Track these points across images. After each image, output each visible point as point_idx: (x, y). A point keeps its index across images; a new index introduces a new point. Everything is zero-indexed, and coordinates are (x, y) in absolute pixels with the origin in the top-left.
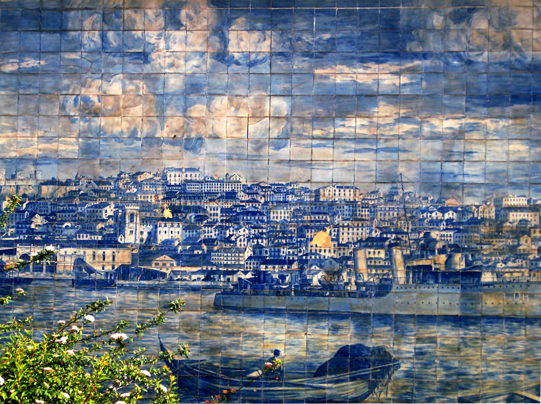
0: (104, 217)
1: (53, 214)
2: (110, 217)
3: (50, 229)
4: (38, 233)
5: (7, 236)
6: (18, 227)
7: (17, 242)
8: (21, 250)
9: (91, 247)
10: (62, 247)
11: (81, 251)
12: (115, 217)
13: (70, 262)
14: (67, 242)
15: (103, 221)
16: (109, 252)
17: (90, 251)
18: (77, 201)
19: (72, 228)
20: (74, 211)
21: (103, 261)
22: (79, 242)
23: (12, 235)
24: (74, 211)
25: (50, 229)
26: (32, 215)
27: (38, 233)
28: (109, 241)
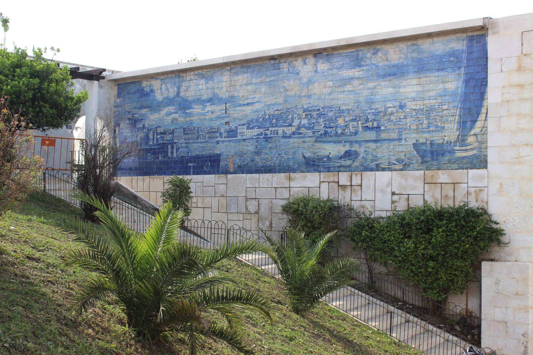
8: (270, 129)
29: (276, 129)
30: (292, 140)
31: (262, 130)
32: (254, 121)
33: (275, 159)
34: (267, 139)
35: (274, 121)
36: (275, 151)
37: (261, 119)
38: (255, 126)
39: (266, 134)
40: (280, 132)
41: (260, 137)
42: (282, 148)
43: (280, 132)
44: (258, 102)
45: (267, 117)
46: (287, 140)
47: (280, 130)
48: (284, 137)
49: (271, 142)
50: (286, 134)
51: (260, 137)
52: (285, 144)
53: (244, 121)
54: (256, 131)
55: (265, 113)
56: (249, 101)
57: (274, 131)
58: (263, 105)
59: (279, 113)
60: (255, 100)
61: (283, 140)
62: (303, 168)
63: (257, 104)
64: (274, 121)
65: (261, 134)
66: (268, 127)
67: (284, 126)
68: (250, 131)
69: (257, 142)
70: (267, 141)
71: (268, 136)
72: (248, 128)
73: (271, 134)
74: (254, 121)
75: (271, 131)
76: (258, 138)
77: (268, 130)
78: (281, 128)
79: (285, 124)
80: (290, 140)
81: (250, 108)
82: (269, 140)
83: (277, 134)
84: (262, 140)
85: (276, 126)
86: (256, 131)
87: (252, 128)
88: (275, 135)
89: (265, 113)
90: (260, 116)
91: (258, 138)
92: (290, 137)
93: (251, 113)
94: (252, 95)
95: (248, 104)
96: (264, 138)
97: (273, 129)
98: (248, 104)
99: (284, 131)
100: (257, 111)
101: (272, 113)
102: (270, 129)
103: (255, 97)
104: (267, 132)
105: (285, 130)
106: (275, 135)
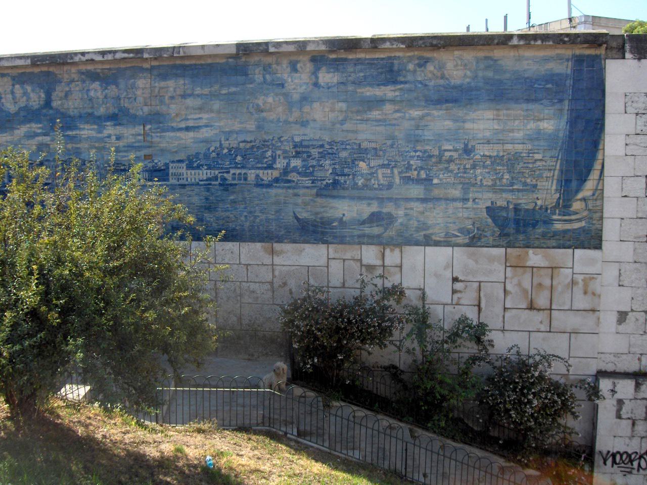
8: (232, 171)
26: (236, 156)
31: (217, 172)
32: (201, 156)
37: (214, 155)
38: (202, 165)
41: (213, 183)
45: (225, 151)
51: (213, 183)
53: (182, 156)
55: (221, 144)
64: (239, 158)
65: (216, 178)
68: (193, 172)
71: (227, 182)
72: (190, 167)
74: (201, 156)
76: (210, 184)
77: (228, 172)
87: (199, 167)
90: (212, 148)
93: (194, 142)
96: (220, 185)
100: (206, 141)
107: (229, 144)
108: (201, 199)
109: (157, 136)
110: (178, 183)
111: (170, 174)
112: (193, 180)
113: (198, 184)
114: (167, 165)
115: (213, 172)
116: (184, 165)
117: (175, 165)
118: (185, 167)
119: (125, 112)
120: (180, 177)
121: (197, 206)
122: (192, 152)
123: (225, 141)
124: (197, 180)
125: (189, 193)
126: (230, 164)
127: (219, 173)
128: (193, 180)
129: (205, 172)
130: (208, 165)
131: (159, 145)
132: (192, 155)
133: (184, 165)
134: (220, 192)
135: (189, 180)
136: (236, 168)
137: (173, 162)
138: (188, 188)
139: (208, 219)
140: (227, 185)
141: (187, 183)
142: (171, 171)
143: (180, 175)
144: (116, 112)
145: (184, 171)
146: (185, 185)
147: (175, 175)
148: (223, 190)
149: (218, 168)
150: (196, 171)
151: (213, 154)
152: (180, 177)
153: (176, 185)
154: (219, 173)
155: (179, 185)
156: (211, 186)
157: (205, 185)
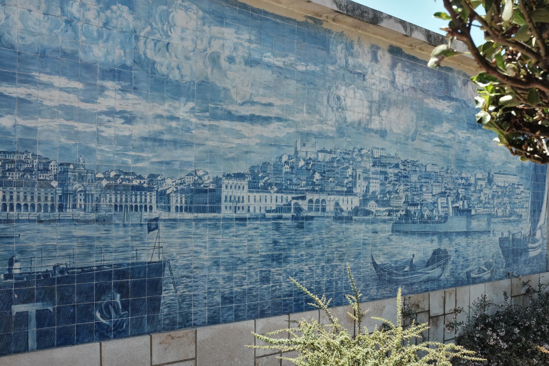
0: (348, 176)
1: (324, 172)
2: (350, 176)
3: (323, 182)
4: (317, 185)
5: (301, 187)
6: (307, 181)
7: (307, 190)
8: (309, 196)
9: (342, 195)
10: (329, 195)
11: (337, 197)
12: (352, 176)
13: (333, 203)
14: (331, 191)
15: (347, 178)
16: (350, 198)
17: (341, 197)
18: (335, 164)
19: (334, 182)
20: (334, 171)
21: (348, 204)
22: (337, 192)
23: (304, 187)
24: (334, 171)
25: (323, 182)
26: (314, 172)
27: (317, 185)
28: (350, 192)
29: (322, 197)
30: (353, 227)
31: (290, 197)
32: (270, 169)
33: (319, 271)
34: (301, 221)
35: (317, 176)
36: (319, 252)
38: (270, 185)
39: (299, 209)
40: (330, 207)
41: (285, 215)
42: (335, 245)
43: (330, 207)
44: (279, 119)
45: (302, 163)
46: (344, 226)
47: (330, 201)
48: (338, 218)
49: (310, 231)
50: (342, 211)
51: (285, 215)
52: (341, 236)
53: (244, 168)
54: (272, 200)
55: (296, 152)
56: (257, 111)
57: (318, 201)
58: (292, 130)
59: (328, 157)
60: (274, 112)
61: (336, 226)
62: (373, 292)
63: (275, 125)
64: (317, 176)
66: (302, 192)
67: (339, 193)
68: (258, 195)
69: (277, 227)
70: (300, 226)
72: (253, 187)
73: (310, 209)
75: (311, 201)
76: (280, 218)
77: (303, 198)
78: (332, 197)
79: (339, 189)
80: (348, 226)
81: (258, 129)
82: (306, 223)
83: (324, 210)
84: (289, 222)
85: (322, 191)
86: (272, 200)
87: (265, 188)
88: (320, 213)
89: (296, 152)
90: (285, 158)
91: (280, 218)
92: (349, 219)
93: (261, 145)
94: (264, 96)
95: (252, 119)
96: (294, 218)
97: (315, 197)
98: (252, 119)
99: (337, 204)
100: (275, 144)
101: (313, 156)
102: (309, 196)
103: (270, 105)
104: (300, 202)
105: (341, 203)
106: (320, 213)
107: (307, 152)
108: (267, 244)
109: (204, 126)
110: (235, 215)
111: (223, 199)
112: (258, 211)
113: (264, 218)
114: (217, 181)
115: (285, 196)
116: (245, 183)
117: (231, 182)
118: (246, 187)
119: (148, 66)
120: (239, 205)
121: (261, 256)
122: (257, 159)
123: (301, 147)
124: (263, 211)
125: (251, 233)
126: (307, 185)
127: (293, 198)
128: (258, 211)
129: (274, 196)
130: (280, 184)
131: (207, 143)
132: (258, 166)
133: (245, 183)
134: (293, 230)
135: (252, 209)
136: (313, 191)
137: (228, 176)
138: (250, 225)
139: (277, 277)
140: (303, 218)
141: (248, 216)
142: (225, 192)
143: (239, 201)
144: (129, 63)
145: (244, 193)
146: (244, 219)
147: (230, 201)
148: (298, 227)
149: (291, 191)
150: (261, 194)
151: (287, 166)
152: (239, 205)
153: (231, 219)
154: (293, 198)
155: (237, 219)
156: (281, 221)
157: (274, 219)
